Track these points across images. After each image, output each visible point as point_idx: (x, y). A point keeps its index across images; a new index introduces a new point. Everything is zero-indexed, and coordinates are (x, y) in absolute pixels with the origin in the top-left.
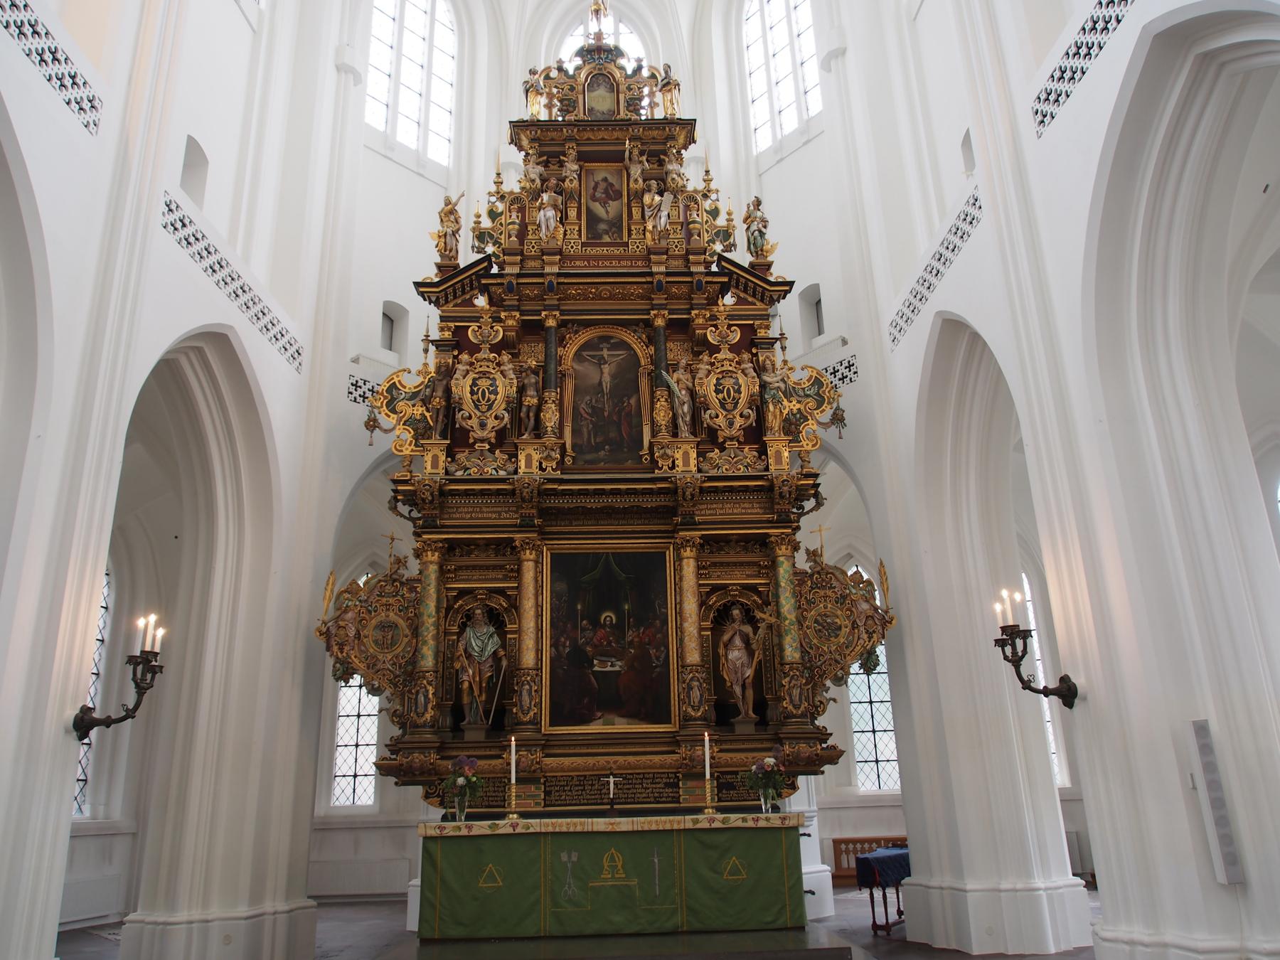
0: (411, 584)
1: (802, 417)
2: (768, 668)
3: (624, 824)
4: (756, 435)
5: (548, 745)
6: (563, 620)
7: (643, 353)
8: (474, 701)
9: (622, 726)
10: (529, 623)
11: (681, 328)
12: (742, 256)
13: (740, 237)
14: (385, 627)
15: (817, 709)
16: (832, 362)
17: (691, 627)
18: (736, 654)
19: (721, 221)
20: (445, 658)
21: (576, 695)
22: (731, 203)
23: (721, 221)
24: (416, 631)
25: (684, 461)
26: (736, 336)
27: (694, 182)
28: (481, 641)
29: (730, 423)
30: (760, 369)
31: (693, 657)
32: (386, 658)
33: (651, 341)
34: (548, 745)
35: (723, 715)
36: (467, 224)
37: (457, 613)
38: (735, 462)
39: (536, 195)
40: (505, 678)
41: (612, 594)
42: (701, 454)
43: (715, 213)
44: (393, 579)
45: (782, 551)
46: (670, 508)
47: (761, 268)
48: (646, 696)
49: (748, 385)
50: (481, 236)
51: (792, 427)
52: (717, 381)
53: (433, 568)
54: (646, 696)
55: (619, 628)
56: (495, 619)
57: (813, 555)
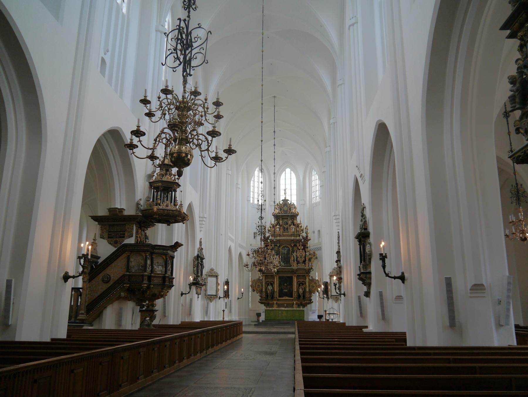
0: (261, 280)
1: (312, 258)
2: (304, 292)
3: (286, 309)
4: (304, 262)
5: (278, 300)
6: (280, 285)
7: (291, 249)
8: (269, 295)
9: (287, 298)
10: (276, 286)
11: (295, 245)
12: (304, 235)
13: (304, 231)
14: (259, 285)
15: (311, 297)
16: (319, 246)
17: (295, 287)
18: (301, 290)
19: (302, 228)
20: (266, 289)
21: (281, 294)
22: (304, 225)
23: (302, 228)
24: (262, 286)
25: (295, 266)
26: (302, 248)
27: (299, 222)
28: (270, 287)
29: (301, 260)
30: (305, 252)
31: (295, 290)
32: (258, 289)
33: (292, 247)
34: (278, 300)
35: (299, 296)
36: (267, 229)
37: (267, 284)
38: (301, 266)
39: (276, 225)
40: (273, 292)
41: (285, 281)
42: (297, 264)
43: (301, 227)
44: (259, 279)
45: (307, 277)
46: (293, 272)
47: (307, 237)
48: (290, 294)
49: (304, 255)
50: (269, 231)
51: (310, 260)
52: (299, 254)
53: (264, 279)
54: (290, 294)
55: (287, 286)
56: (272, 285)
57: (312, 277)
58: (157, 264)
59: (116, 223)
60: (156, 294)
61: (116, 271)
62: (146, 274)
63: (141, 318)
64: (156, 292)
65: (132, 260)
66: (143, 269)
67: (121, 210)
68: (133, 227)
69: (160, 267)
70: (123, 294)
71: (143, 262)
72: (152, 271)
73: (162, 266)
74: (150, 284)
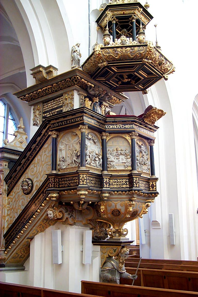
58: (115, 153)
59: (50, 96)
60: (119, 212)
61: (38, 171)
62: (83, 168)
63: (102, 258)
64: (119, 207)
65: (61, 146)
66: (79, 161)
67: (49, 70)
68: (72, 95)
69: (121, 157)
70: (51, 213)
71: (78, 147)
72: (104, 165)
73: (126, 155)
74: (102, 192)
